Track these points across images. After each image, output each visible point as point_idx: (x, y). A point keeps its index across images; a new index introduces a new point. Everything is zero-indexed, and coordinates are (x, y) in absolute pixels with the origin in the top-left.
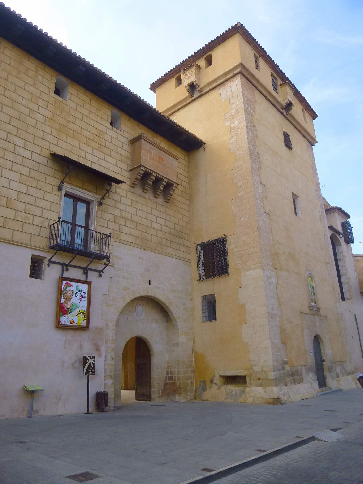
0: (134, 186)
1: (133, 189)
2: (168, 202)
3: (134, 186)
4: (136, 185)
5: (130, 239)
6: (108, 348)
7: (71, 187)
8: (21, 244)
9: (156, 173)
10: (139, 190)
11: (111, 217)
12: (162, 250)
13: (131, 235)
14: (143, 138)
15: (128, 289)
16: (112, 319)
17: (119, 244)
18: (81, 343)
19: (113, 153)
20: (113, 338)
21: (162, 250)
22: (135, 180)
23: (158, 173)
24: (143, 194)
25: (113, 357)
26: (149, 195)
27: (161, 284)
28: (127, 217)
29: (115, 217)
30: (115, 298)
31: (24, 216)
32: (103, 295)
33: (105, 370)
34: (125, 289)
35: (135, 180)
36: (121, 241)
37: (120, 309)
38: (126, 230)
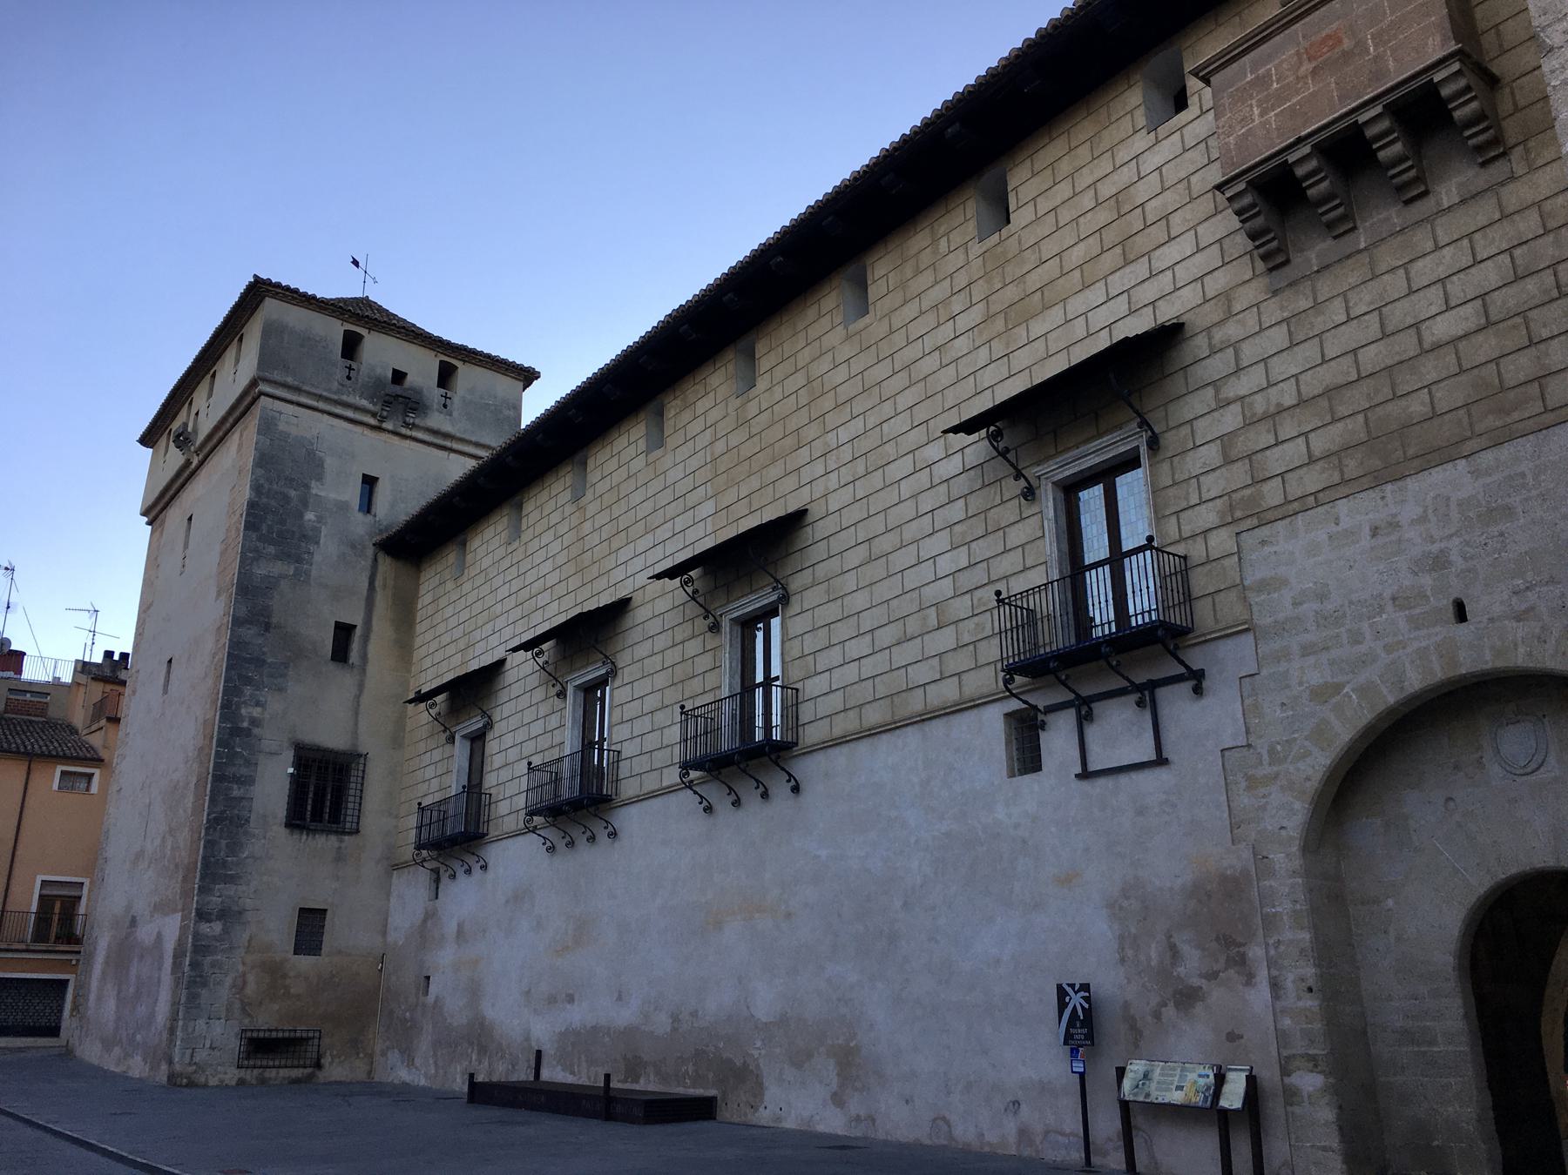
0: (1280, 259)
1: (1286, 270)
2: (1504, 154)
3: (1280, 259)
4: (1279, 250)
5: (1312, 480)
6: (1282, 948)
7: (1057, 463)
8: (973, 700)
9: (1300, 140)
10: (1314, 251)
11: (1211, 454)
12: (1516, 416)
13: (1312, 460)
14: (1209, 73)
15: (1338, 688)
16: (1283, 832)
17: (1265, 532)
18: (1172, 940)
19: (1176, 219)
20: (1298, 907)
21: (1516, 416)
22: (1257, 243)
23: (1303, 134)
24: (1346, 244)
25: (1311, 982)
26: (1382, 217)
27: (1538, 589)
28: (1278, 405)
29: (1226, 440)
30: (1279, 747)
31: (973, 626)
32: (1227, 753)
33: (1282, 1037)
34: (1322, 694)
35: (1257, 243)
36: (1270, 516)
37: (1308, 784)
38: (1276, 461)
